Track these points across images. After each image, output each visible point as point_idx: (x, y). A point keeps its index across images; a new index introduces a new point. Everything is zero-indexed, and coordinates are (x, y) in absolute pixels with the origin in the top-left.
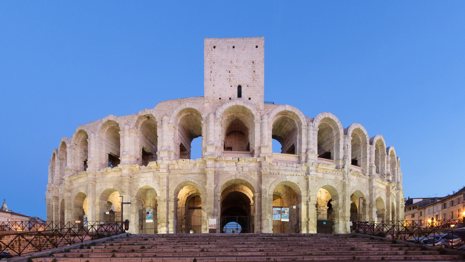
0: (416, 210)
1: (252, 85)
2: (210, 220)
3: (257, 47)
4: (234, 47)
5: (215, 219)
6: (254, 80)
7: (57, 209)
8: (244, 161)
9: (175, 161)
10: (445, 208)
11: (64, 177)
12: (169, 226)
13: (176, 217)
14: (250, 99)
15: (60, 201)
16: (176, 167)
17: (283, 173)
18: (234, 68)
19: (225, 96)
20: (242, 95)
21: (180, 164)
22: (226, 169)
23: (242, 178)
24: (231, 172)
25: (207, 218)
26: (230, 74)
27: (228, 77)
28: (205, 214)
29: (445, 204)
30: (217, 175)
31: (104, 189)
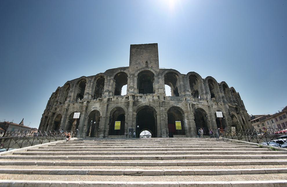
24: (142, 102)
30: (134, 104)
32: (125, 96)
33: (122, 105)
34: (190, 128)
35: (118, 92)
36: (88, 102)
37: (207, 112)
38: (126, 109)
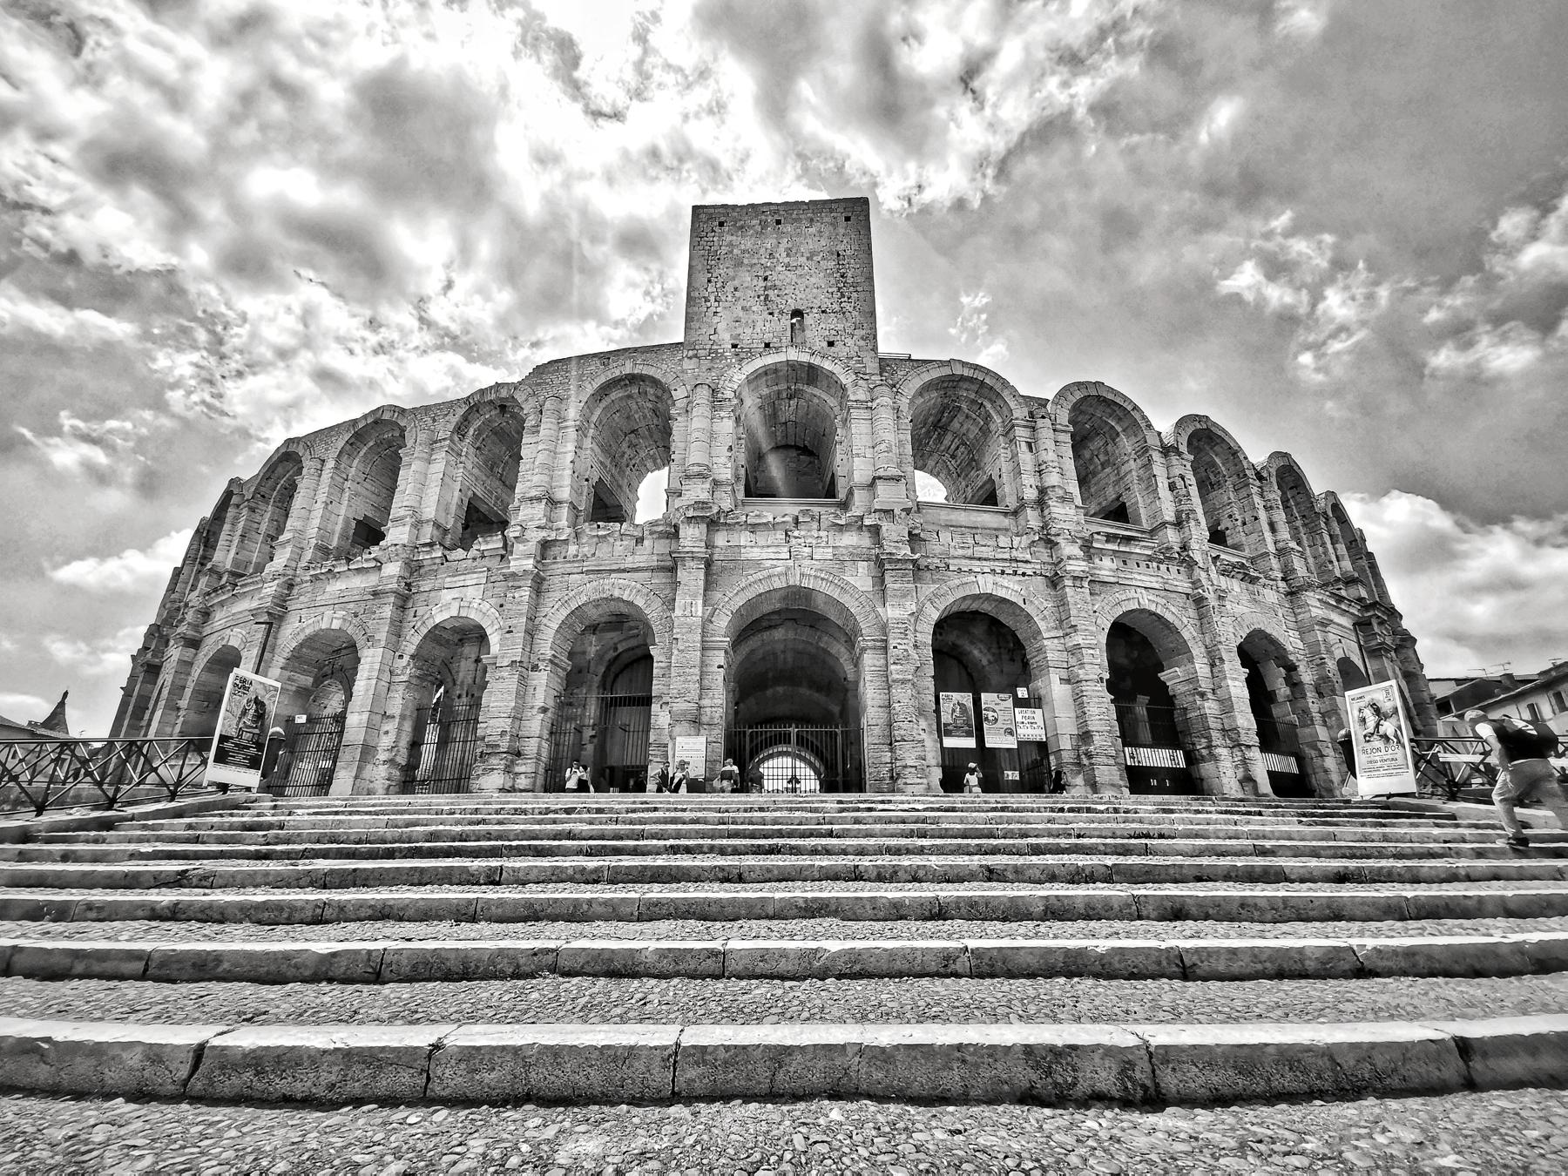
1: (836, 307)
6: (843, 296)
8: (815, 525)
14: (831, 344)
17: (965, 565)
32: (653, 524)
33: (633, 591)
34: (1085, 736)
35: (606, 507)
36: (414, 568)
37: (1189, 633)
38: (653, 612)
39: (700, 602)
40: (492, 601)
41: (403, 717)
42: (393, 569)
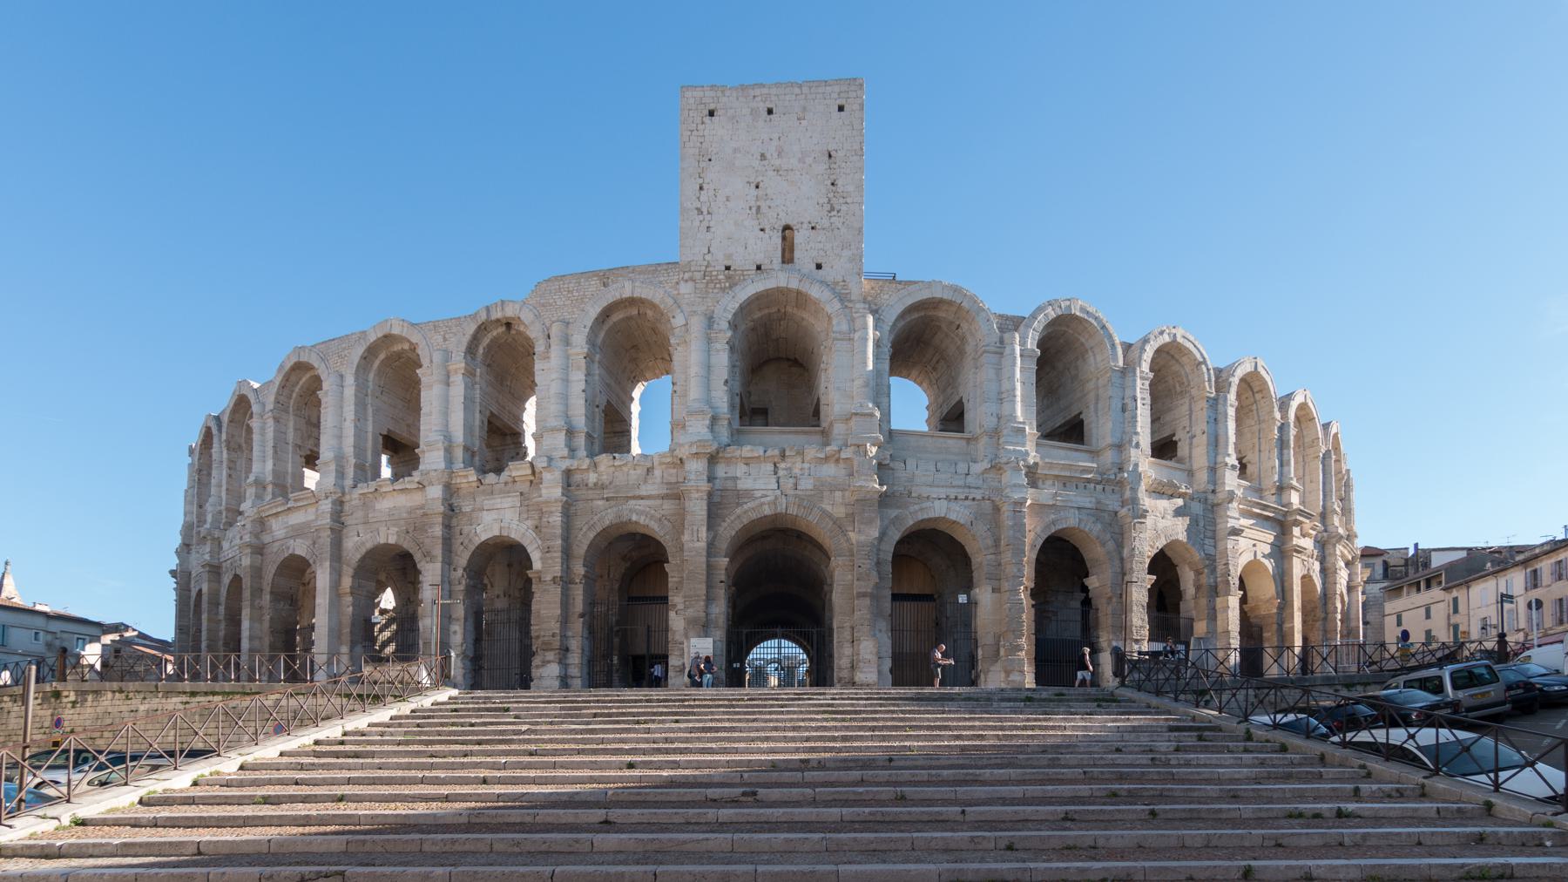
0: (1436, 593)
1: (827, 225)
2: (693, 641)
3: (841, 109)
4: (770, 112)
5: (710, 640)
6: (832, 209)
7: (214, 603)
9: (587, 461)
10: (1535, 586)
11: (243, 507)
12: (570, 661)
13: (591, 630)
14: (819, 267)
15: (226, 580)
16: (592, 478)
18: (771, 173)
19: (743, 260)
20: (797, 254)
21: (602, 468)
22: (741, 485)
23: (793, 511)
24: (758, 494)
25: (687, 637)
26: (760, 192)
27: (752, 203)
28: (676, 622)
29: (1535, 571)
31: (369, 545)
33: (646, 515)
39: (704, 529)
40: (529, 523)
41: (466, 619)
42: (435, 492)
